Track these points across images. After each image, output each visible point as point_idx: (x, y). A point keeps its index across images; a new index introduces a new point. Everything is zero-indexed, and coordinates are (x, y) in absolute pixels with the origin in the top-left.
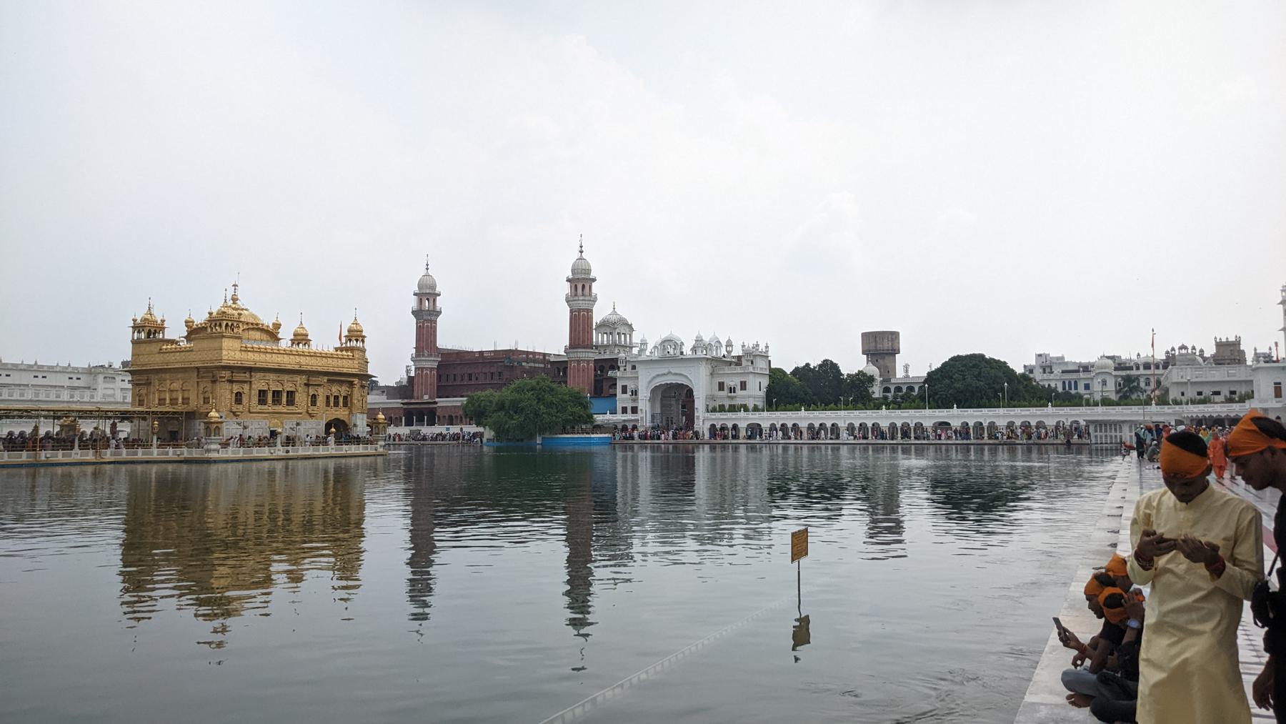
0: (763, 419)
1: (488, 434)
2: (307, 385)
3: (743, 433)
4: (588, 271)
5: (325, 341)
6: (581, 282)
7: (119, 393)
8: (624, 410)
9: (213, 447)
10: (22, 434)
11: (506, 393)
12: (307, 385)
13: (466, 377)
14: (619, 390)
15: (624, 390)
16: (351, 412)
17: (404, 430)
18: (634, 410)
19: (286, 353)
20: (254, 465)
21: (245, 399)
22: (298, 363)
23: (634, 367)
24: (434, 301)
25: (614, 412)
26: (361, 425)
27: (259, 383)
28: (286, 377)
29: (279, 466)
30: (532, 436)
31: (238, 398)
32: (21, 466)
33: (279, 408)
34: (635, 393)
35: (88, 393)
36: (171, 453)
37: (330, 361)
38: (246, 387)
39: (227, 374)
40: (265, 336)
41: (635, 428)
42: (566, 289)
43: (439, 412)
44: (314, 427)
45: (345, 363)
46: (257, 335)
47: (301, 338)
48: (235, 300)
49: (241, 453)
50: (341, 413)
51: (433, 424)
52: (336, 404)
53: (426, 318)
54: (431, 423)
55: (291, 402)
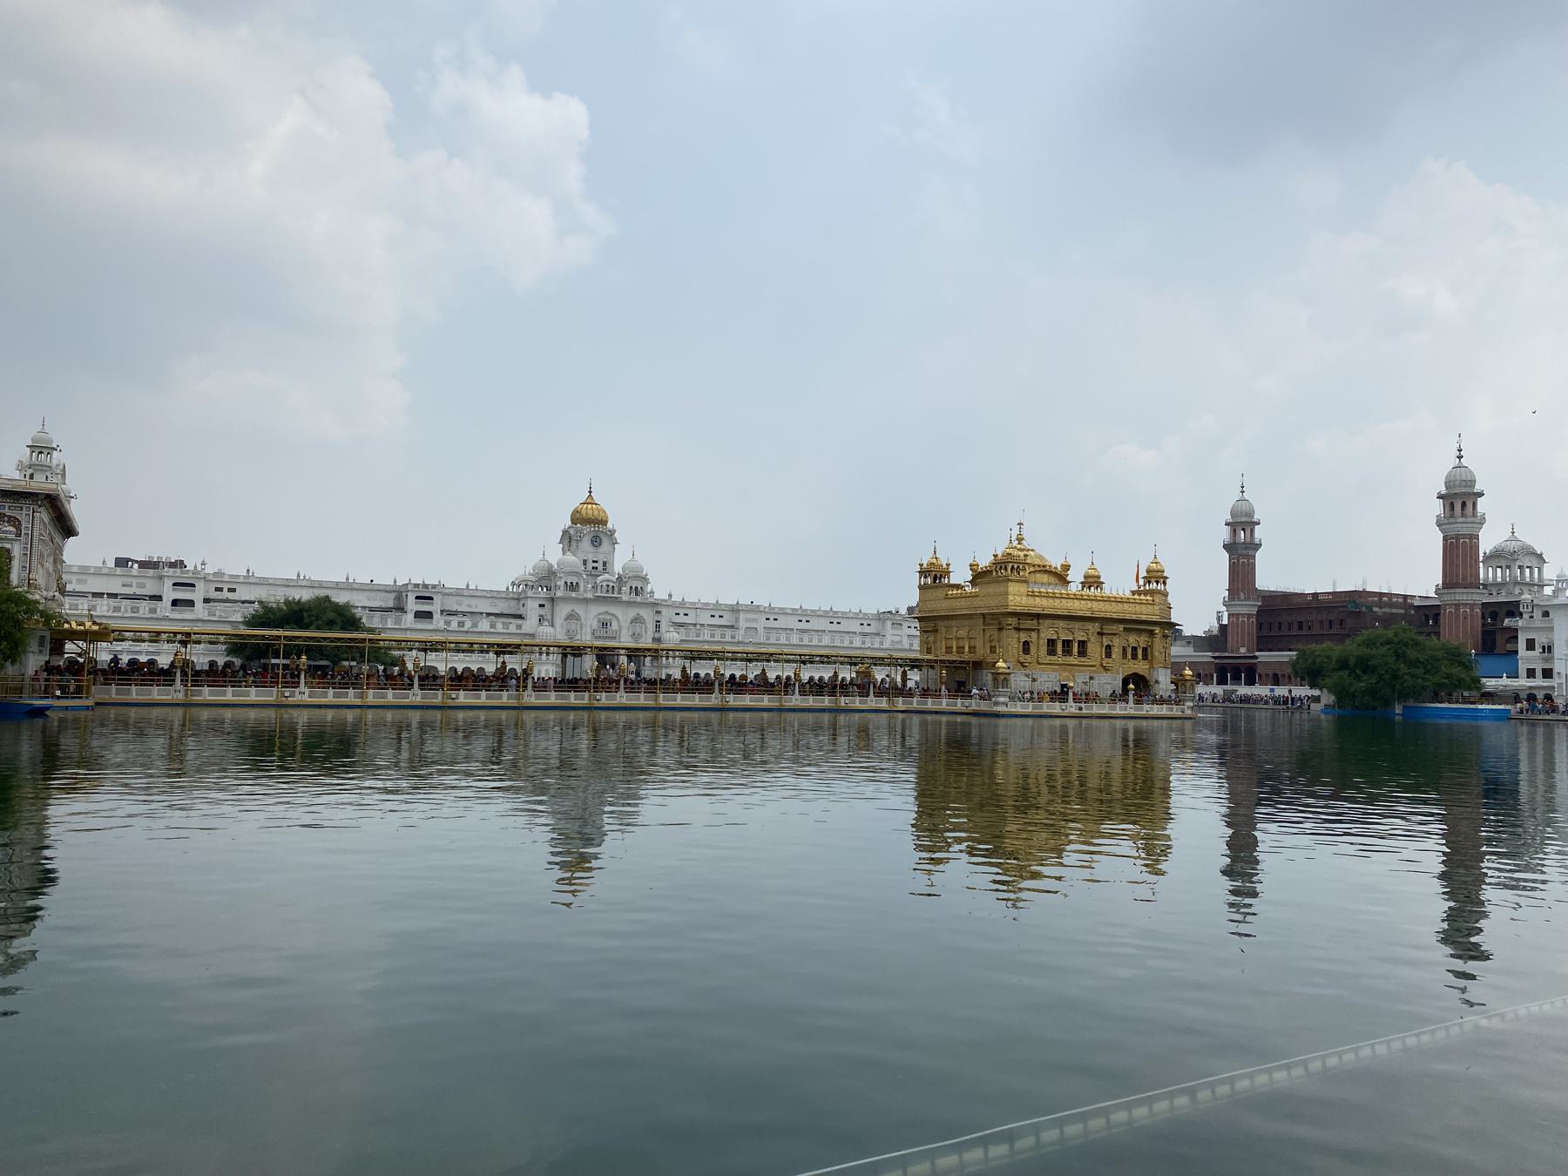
1: (1327, 698)
2: (1101, 634)
4: (1472, 482)
5: (1120, 583)
6: (1460, 500)
7: (907, 639)
8: (1531, 673)
9: (1001, 699)
10: (821, 679)
11: (1352, 648)
12: (1101, 634)
13: (1296, 626)
14: (1522, 645)
15: (1531, 645)
16: (1152, 666)
17: (1218, 690)
18: (1548, 674)
19: (1076, 598)
20: (1046, 722)
21: (1033, 648)
22: (1090, 609)
23: (1546, 614)
24: (1252, 531)
25: (1514, 675)
26: (1163, 682)
27: (1048, 632)
28: (1077, 625)
29: (1071, 723)
30: (1388, 703)
31: (1026, 647)
32: (823, 710)
33: (1071, 660)
34: (1548, 649)
35: (877, 639)
36: (959, 704)
37: (1126, 606)
38: (1034, 635)
39: (1013, 621)
40: (1052, 579)
41: (1549, 697)
42: (1438, 508)
43: (1259, 670)
44: (1108, 682)
45: (1144, 608)
46: (1045, 578)
47: (1092, 581)
48: (1020, 540)
49: (1030, 708)
50: (1140, 667)
52: (1134, 656)
53: (1241, 554)
54: (1251, 682)
55: (1083, 652)
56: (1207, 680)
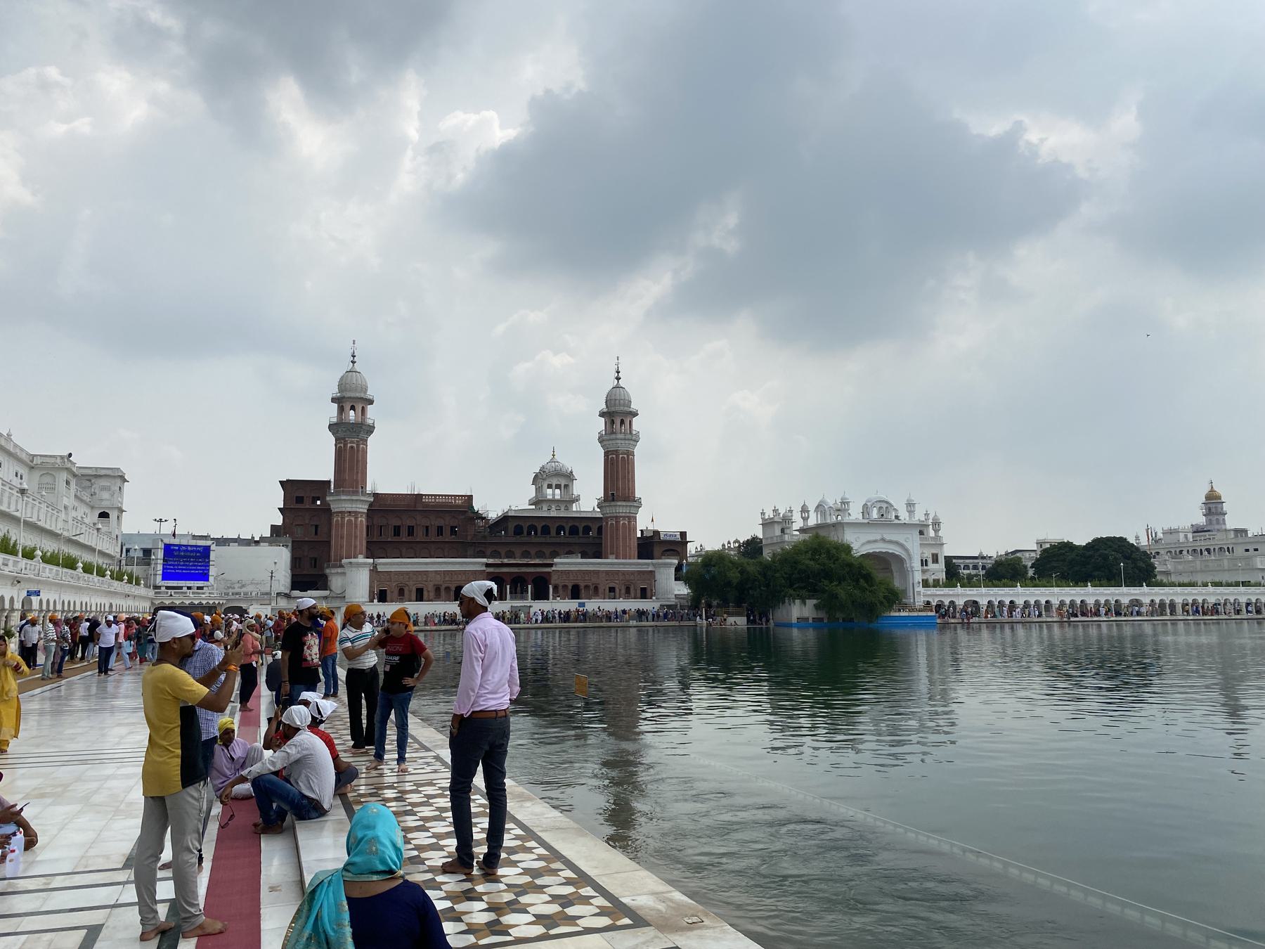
0: (981, 595)
3: (1179, 609)
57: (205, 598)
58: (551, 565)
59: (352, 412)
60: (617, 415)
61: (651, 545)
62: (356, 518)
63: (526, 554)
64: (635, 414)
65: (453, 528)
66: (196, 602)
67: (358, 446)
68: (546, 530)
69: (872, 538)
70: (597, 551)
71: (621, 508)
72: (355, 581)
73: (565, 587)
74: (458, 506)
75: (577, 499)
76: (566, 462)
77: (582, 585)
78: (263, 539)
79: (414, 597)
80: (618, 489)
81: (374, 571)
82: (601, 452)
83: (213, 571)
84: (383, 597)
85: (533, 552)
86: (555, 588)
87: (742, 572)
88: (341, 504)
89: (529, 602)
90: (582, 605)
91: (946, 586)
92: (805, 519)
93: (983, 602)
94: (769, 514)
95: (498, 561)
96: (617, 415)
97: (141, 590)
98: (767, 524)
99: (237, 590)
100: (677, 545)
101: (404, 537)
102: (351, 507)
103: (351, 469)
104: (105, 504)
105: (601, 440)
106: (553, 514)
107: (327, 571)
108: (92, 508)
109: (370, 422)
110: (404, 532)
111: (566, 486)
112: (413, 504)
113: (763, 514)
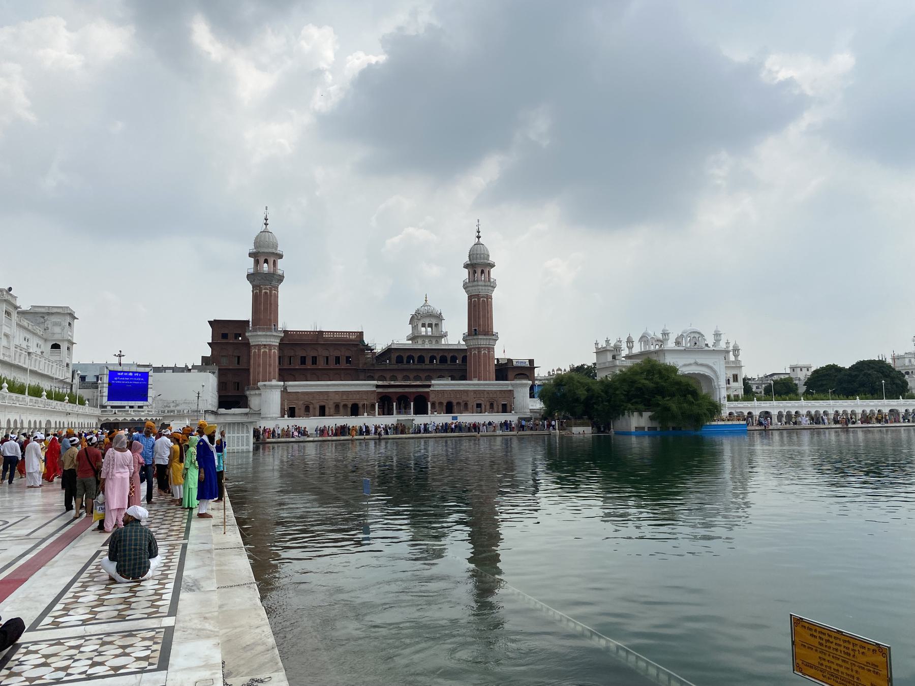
0: (773, 407)
24: (275, 263)
43: (432, 398)
51: (425, 412)
56: (371, 410)
57: (143, 415)
58: (429, 386)
59: (265, 265)
60: (478, 265)
61: (505, 370)
62: (270, 350)
63: (406, 378)
64: (492, 266)
65: (348, 358)
66: (136, 419)
67: (271, 292)
68: (421, 360)
69: (688, 363)
70: (462, 375)
71: (482, 341)
72: (269, 400)
73: (441, 403)
74: (351, 340)
75: (445, 335)
76: (436, 306)
77: (455, 402)
78: (194, 367)
79: (317, 412)
80: (479, 325)
81: (284, 391)
82: (465, 297)
83: (151, 393)
84: (292, 413)
85: (412, 376)
86: (433, 405)
87: (588, 390)
88: (257, 338)
89: (412, 416)
90: (455, 418)
91: (745, 400)
92: (630, 348)
93: (774, 413)
94: (602, 344)
95: (385, 383)
96: (478, 265)
97: (87, 409)
98: (600, 352)
99: (172, 408)
100: (526, 371)
101: (309, 365)
102: (265, 341)
103: (266, 309)
104: (57, 337)
105: (466, 286)
106: (427, 346)
107: (248, 393)
108: (46, 340)
109: (280, 272)
110: (309, 361)
111: (436, 325)
112: (317, 339)
113: (597, 344)
